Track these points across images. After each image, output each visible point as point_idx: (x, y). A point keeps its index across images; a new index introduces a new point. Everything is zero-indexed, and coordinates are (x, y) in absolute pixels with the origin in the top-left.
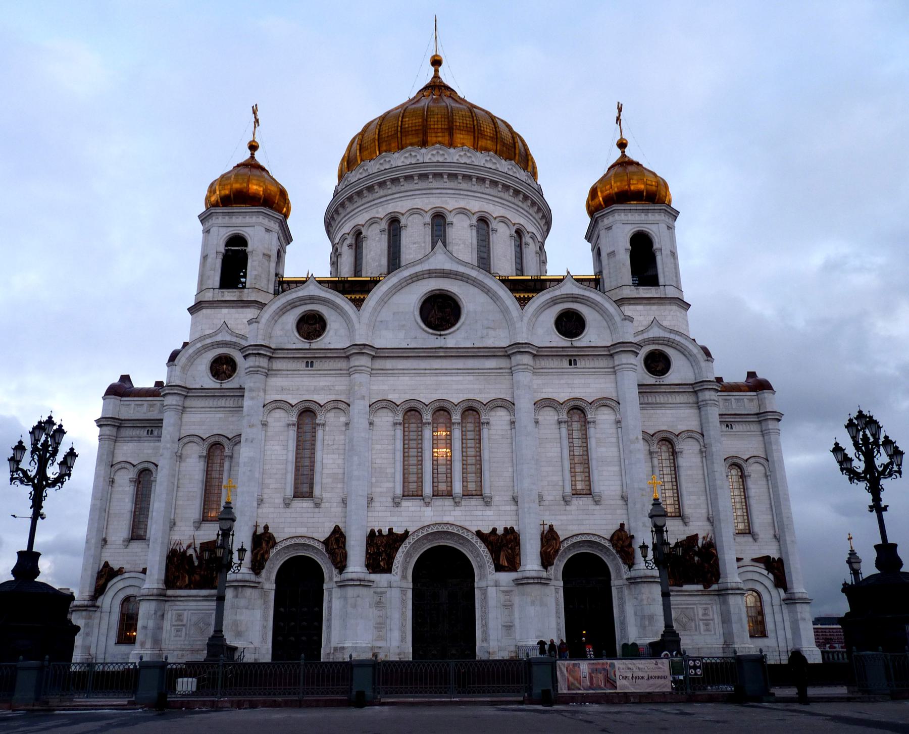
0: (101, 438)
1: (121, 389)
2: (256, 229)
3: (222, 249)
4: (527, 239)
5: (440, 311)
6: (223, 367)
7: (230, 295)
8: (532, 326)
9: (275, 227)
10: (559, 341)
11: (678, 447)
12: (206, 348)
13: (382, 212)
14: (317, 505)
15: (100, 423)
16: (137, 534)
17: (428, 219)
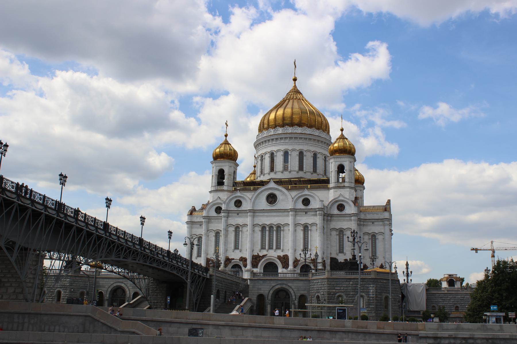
0: (188, 227)
1: (193, 211)
2: (226, 166)
3: (217, 174)
4: (318, 156)
5: (272, 199)
6: (218, 210)
7: (219, 188)
8: (295, 202)
9: (232, 165)
10: (303, 207)
11: (345, 233)
12: (214, 205)
13: (269, 149)
14: (240, 251)
15: (187, 223)
16: (199, 255)
17: (282, 153)
